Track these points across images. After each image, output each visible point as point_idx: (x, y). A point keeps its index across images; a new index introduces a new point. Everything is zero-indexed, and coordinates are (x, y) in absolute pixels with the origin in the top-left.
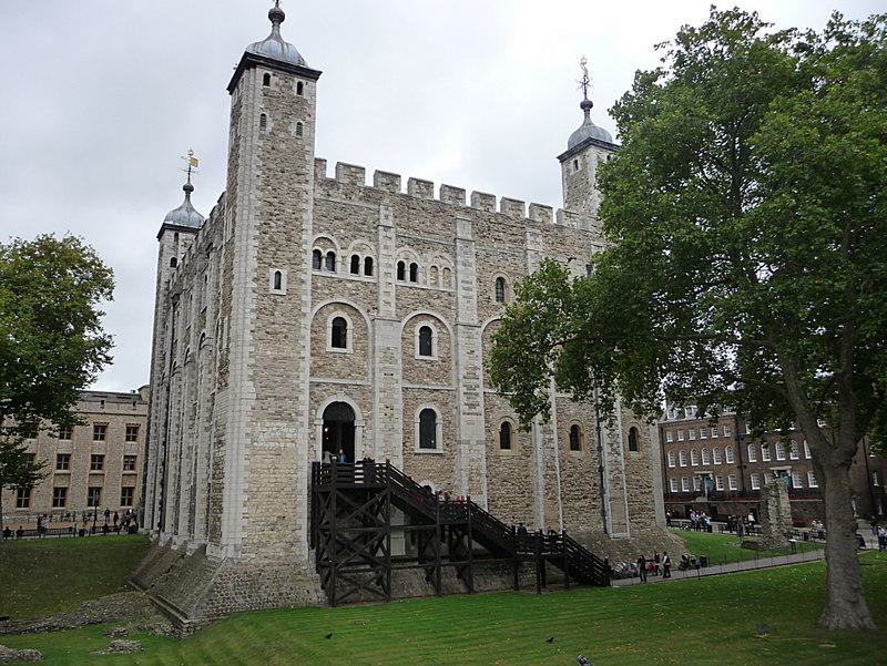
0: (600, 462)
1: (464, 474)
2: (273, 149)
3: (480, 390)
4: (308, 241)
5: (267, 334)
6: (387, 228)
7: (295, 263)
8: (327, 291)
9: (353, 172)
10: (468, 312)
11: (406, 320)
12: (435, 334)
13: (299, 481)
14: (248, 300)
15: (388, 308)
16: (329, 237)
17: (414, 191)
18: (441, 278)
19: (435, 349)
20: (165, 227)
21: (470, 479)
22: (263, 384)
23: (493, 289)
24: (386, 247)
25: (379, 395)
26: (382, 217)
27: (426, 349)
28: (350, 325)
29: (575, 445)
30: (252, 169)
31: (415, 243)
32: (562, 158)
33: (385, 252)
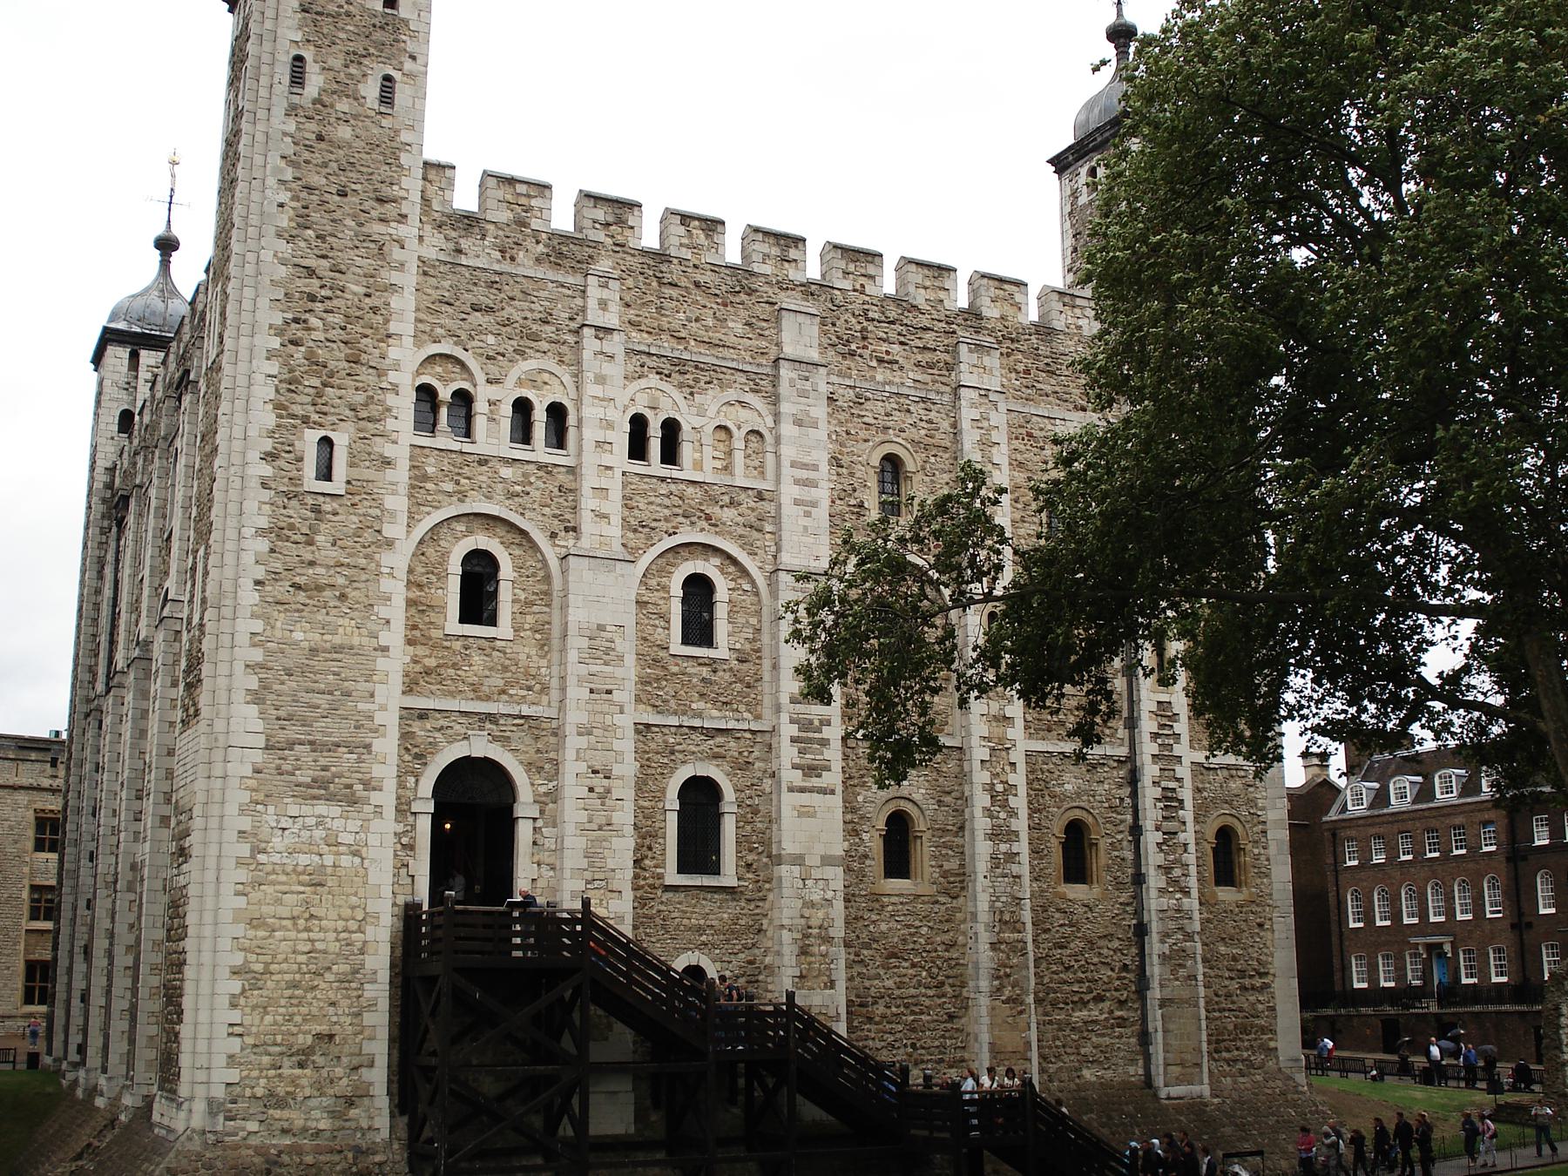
0: (1138, 913)
1: (786, 936)
2: (320, 138)
4: (405, 363)
5: (295, 590)
6: (603, 331)
7: (369, 417)
8: (449, 487)
9: (519, 193)
11: (645, 561)
12: (722, 592)
13: (370, 948)
14: (251, 506)
15: (603, 527)
16: (458, 352)
17: (675, 241)
18: (739, 457)
19: (721, 629)
20: (109, 337)
21: (804, 952)
22: (282, 713)
23: (873, 483)
24: (601, 380)
25: (573, 742)
26: (592, 304)
27: (698, 629)
28: (506, 570)
29: (1076, 866)
30: (270, 196)
31: (674, 368)
32: (1061, 164)
33: (597, 390)
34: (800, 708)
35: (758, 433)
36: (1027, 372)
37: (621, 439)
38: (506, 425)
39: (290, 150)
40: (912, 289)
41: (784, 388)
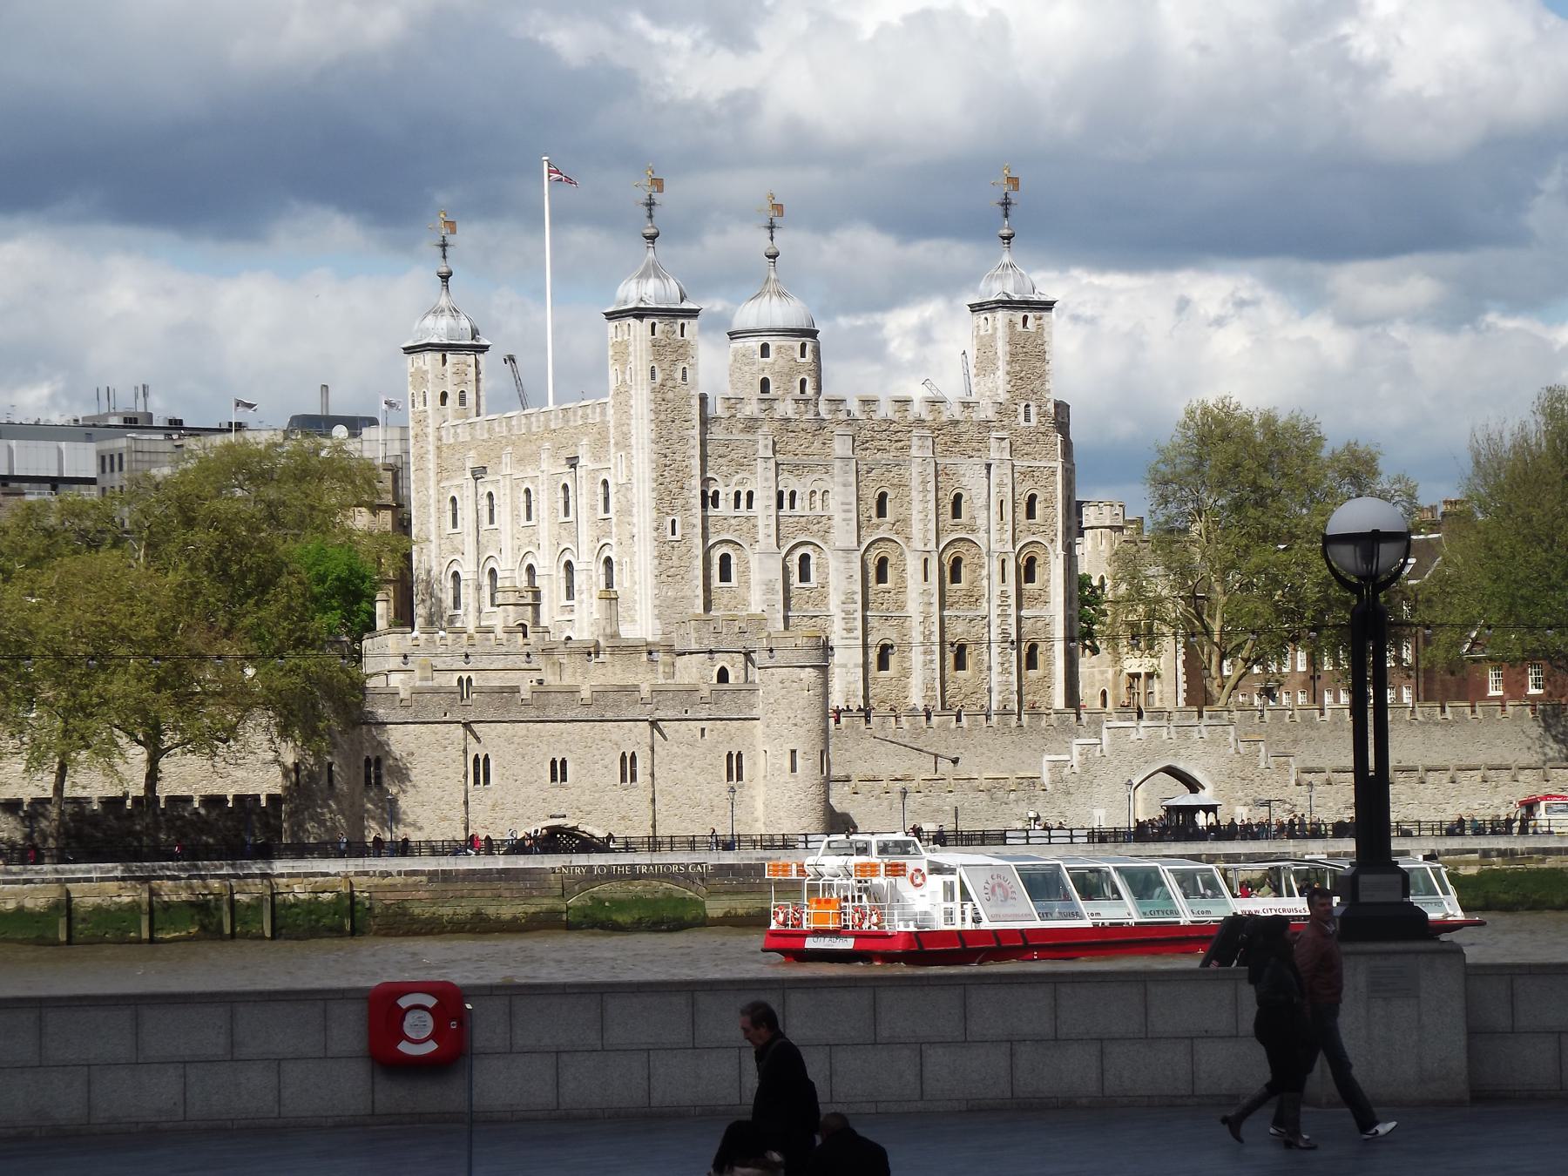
3: (859, 615)
24: (767, 480)
26: (760, 446)
27: (805, 576)
31: (797, 469)
37: (774, 502)
38: (732, 503)
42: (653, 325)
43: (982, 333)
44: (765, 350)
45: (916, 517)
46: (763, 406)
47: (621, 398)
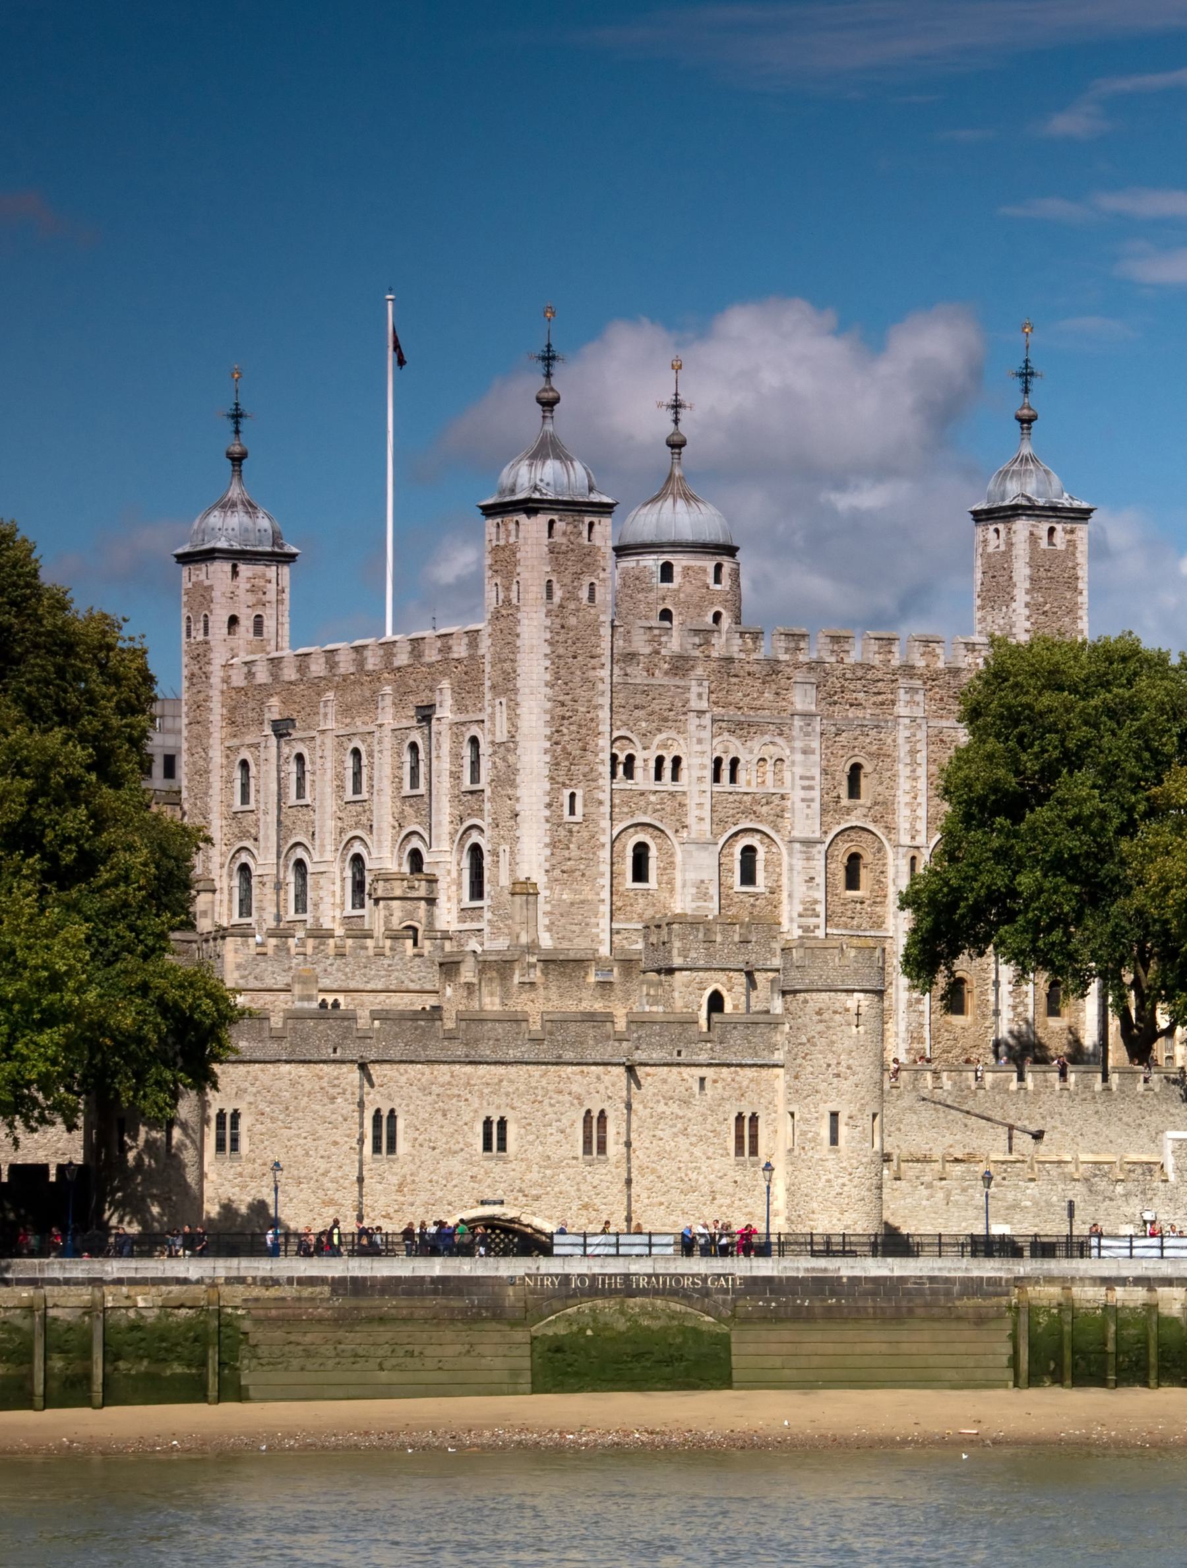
2: (563, 627)
6: (701, 713)
8: (626, 810)
10: (804, 820)
11: (721, 842)
12: (760, 856)
17: (736, 649)
23: (845, 783)
24: (700, 741)
26: (693, 696)
27: (748, 877)
28: (653, 853)
33: (698, 748)
34: (803, 920)
35: (781, 760)
36: (941, 699)
37: (708, 773)
39: (548, 636)
40: (871, 655)
41: (796, 732)
42: (551, 523)
43: (990, 549)
44: (667, 572)
45: (903, 798)
46: (697, 640)
47: (502, 624)
